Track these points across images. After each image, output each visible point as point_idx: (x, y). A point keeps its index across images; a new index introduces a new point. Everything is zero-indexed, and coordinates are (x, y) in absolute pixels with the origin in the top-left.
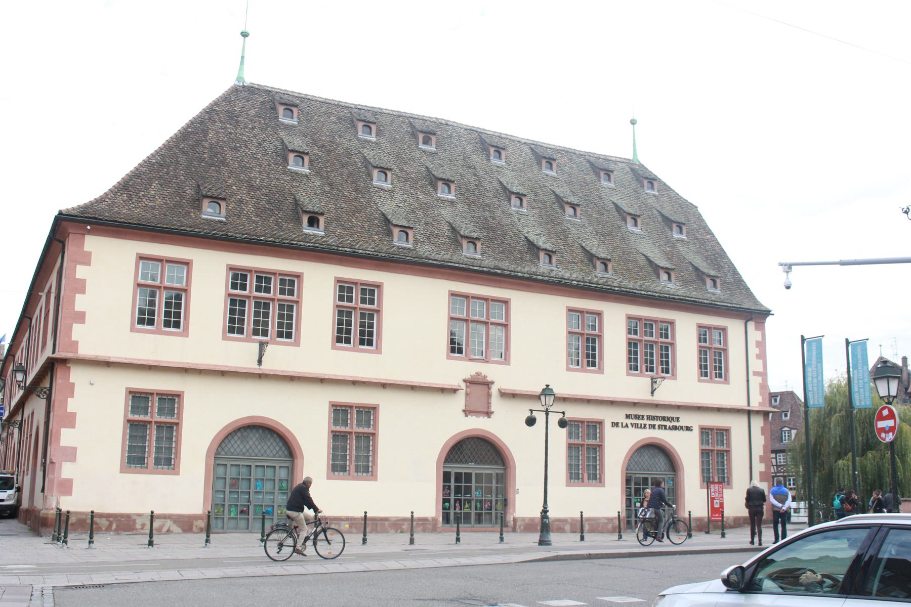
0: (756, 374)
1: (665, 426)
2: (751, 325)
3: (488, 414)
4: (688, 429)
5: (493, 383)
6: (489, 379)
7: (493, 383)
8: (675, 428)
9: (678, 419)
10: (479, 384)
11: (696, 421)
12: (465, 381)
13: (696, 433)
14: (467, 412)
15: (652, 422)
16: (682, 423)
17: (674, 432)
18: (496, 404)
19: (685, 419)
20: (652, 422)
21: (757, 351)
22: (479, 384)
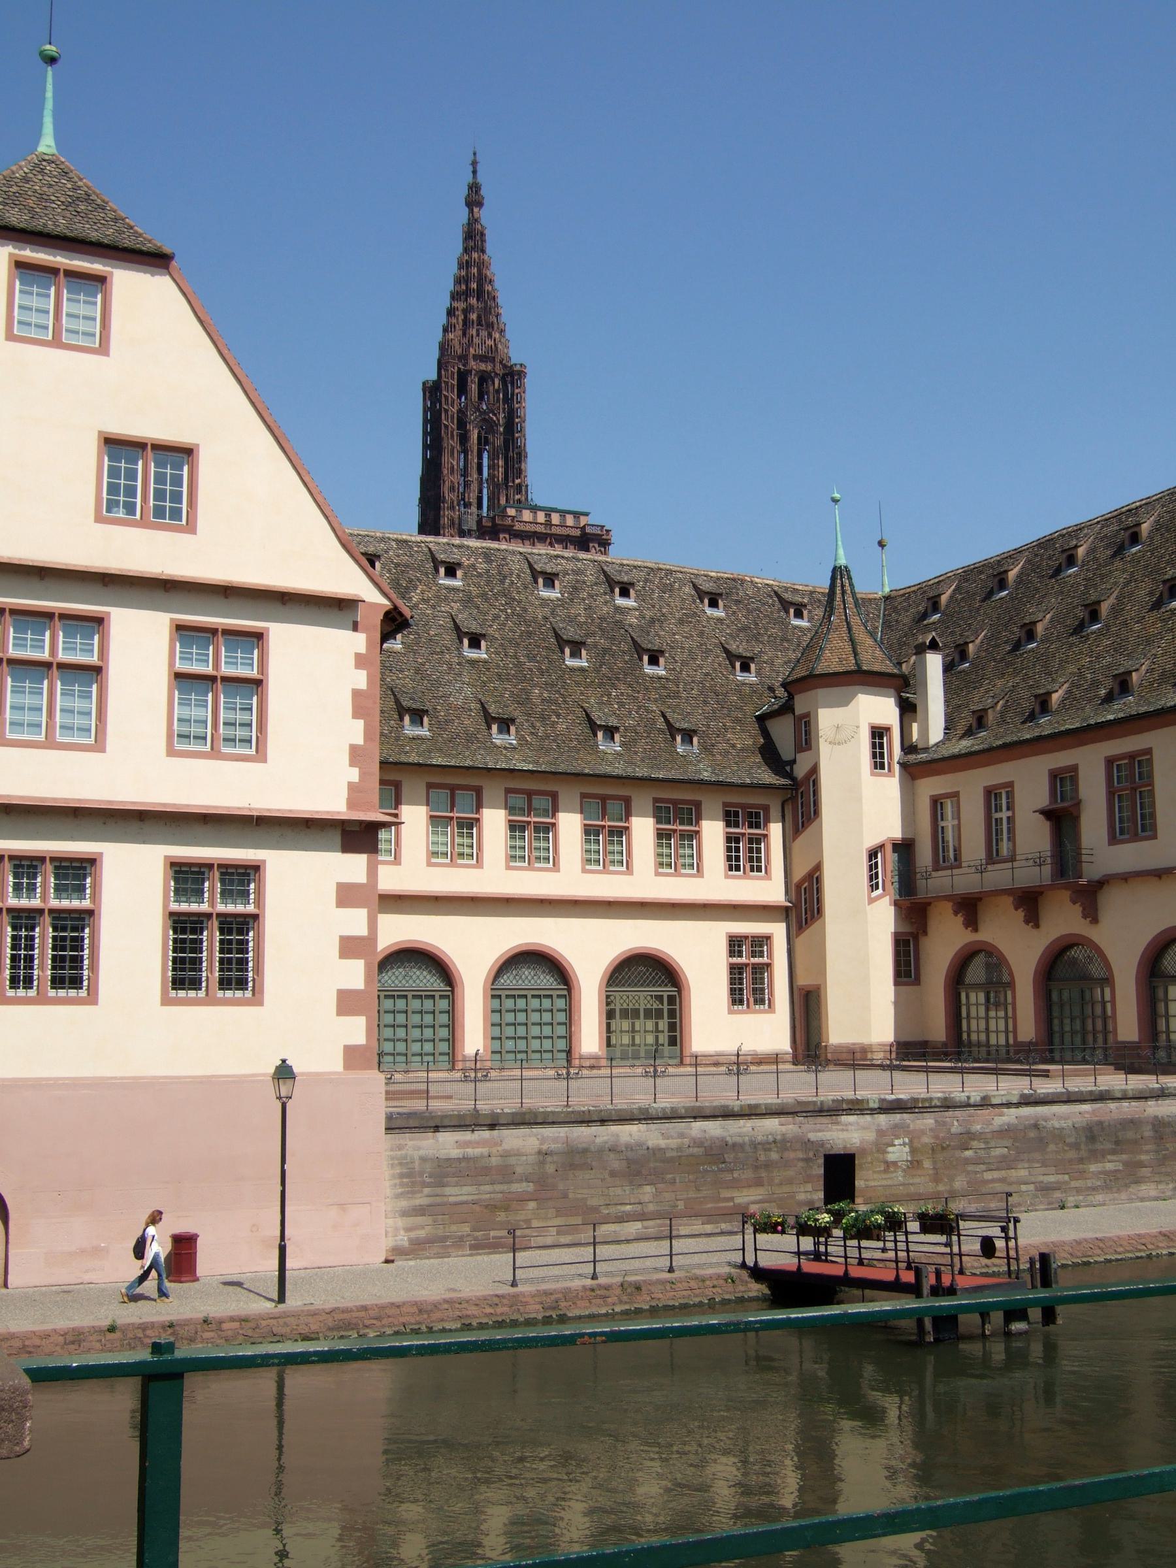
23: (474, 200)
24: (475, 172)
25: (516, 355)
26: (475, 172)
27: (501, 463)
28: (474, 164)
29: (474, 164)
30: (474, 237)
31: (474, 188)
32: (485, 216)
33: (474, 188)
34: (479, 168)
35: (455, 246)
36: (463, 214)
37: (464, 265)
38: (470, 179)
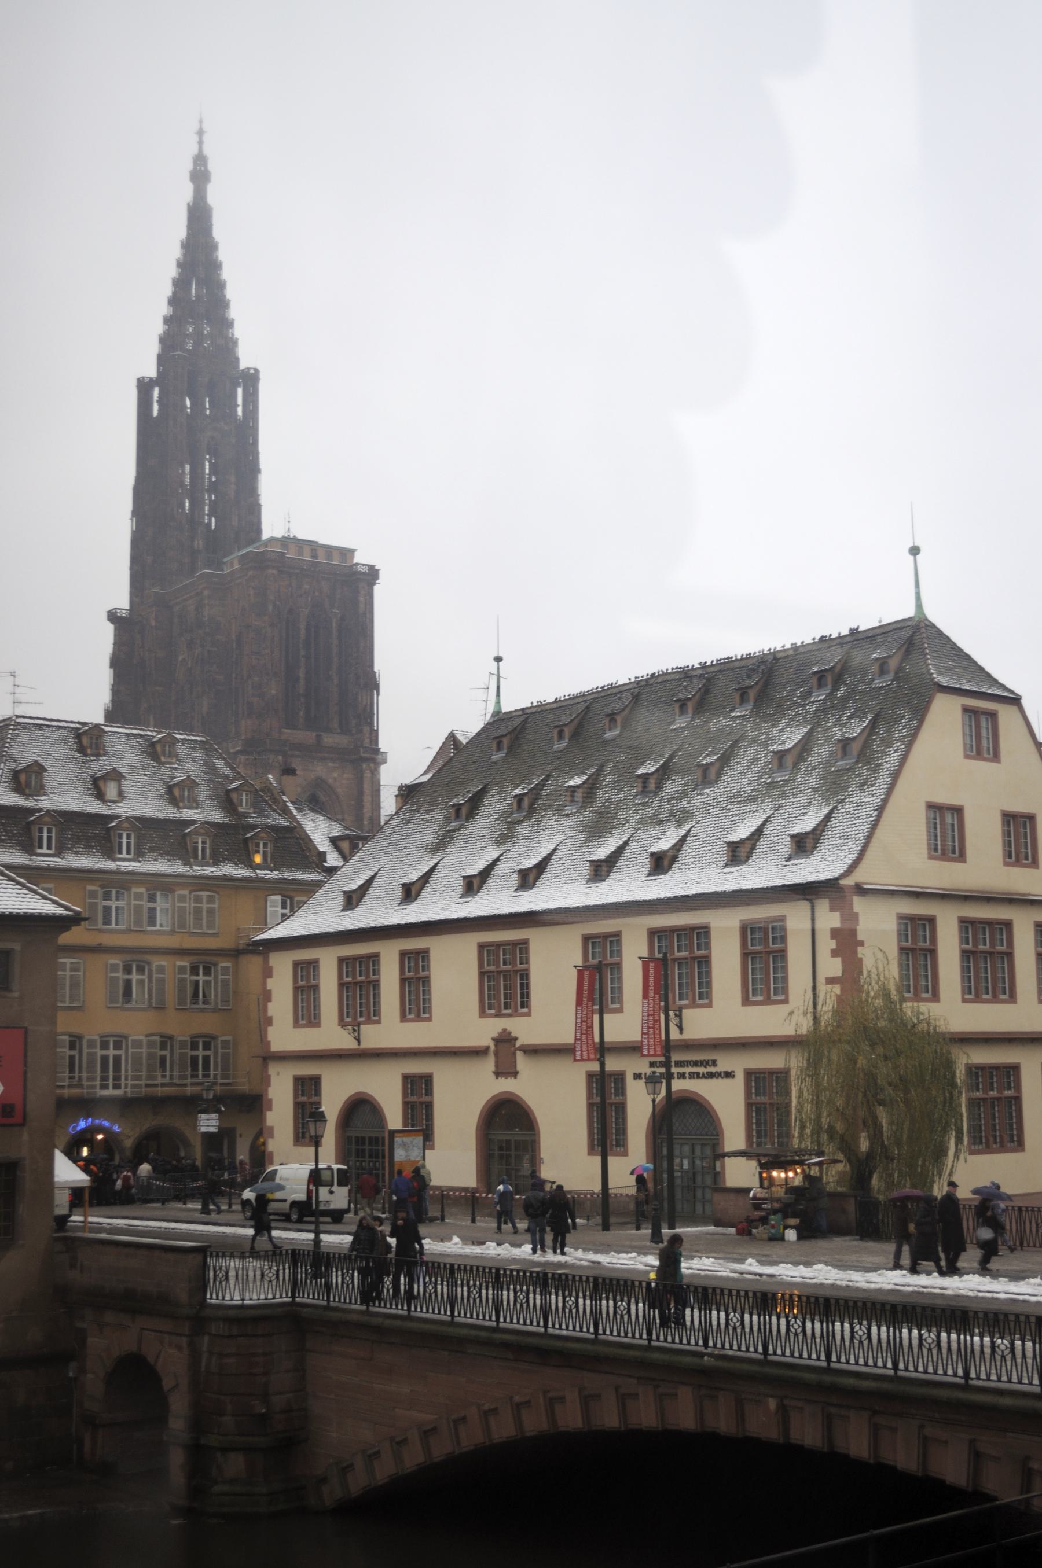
0: (831, 981)
1: (698, 1074)
2: (823, 906)
3: (515, 1074)
4: (729, 1075)
5: (516, 1039)
6: (513, 1035)
7: (516, 1039)
8: (711, 1075)
9: (714, 1063)
10: (505, 1040)
11: (738, 1063)
12: (493, 1039)
13: (740, 1077)
14: (498, 1074)
15: (681, 1070)
16: (721, 1067)
17: (710, 1080)
18: (522, 1062)
19: (725, 1062)
20: (681, 1070)
21: (833, 944)
22: (505, 1040)
23: (200, 176)
24: (200, 143)
25: (246, 359)
26: (200, 143)
27: (233, 479)
28: (200, 133)
29: (200, 133)
30: (199, 217)
31: (200, 160)
32: (214, 196)
33: (200, 160)
34: (205, 138)
35: (179, 230)
36: (186, 193)
37: (188, 246)
38: (195, 150)
